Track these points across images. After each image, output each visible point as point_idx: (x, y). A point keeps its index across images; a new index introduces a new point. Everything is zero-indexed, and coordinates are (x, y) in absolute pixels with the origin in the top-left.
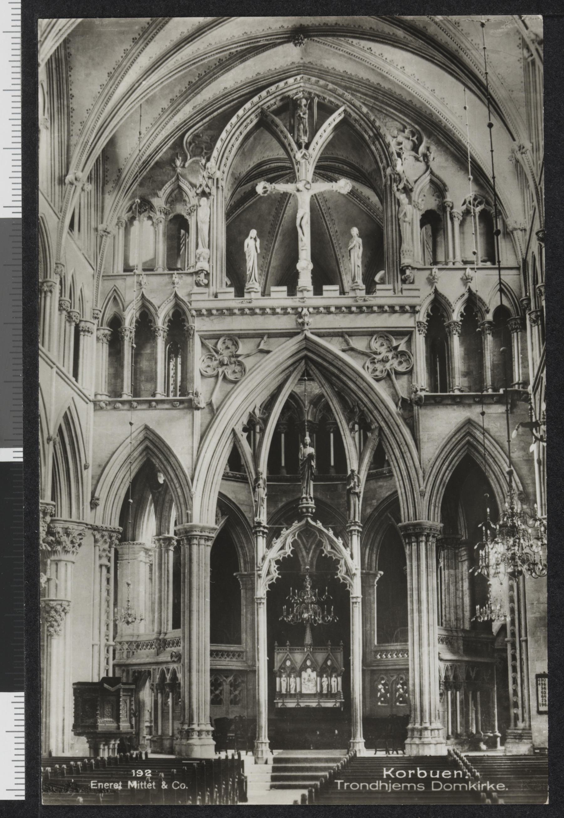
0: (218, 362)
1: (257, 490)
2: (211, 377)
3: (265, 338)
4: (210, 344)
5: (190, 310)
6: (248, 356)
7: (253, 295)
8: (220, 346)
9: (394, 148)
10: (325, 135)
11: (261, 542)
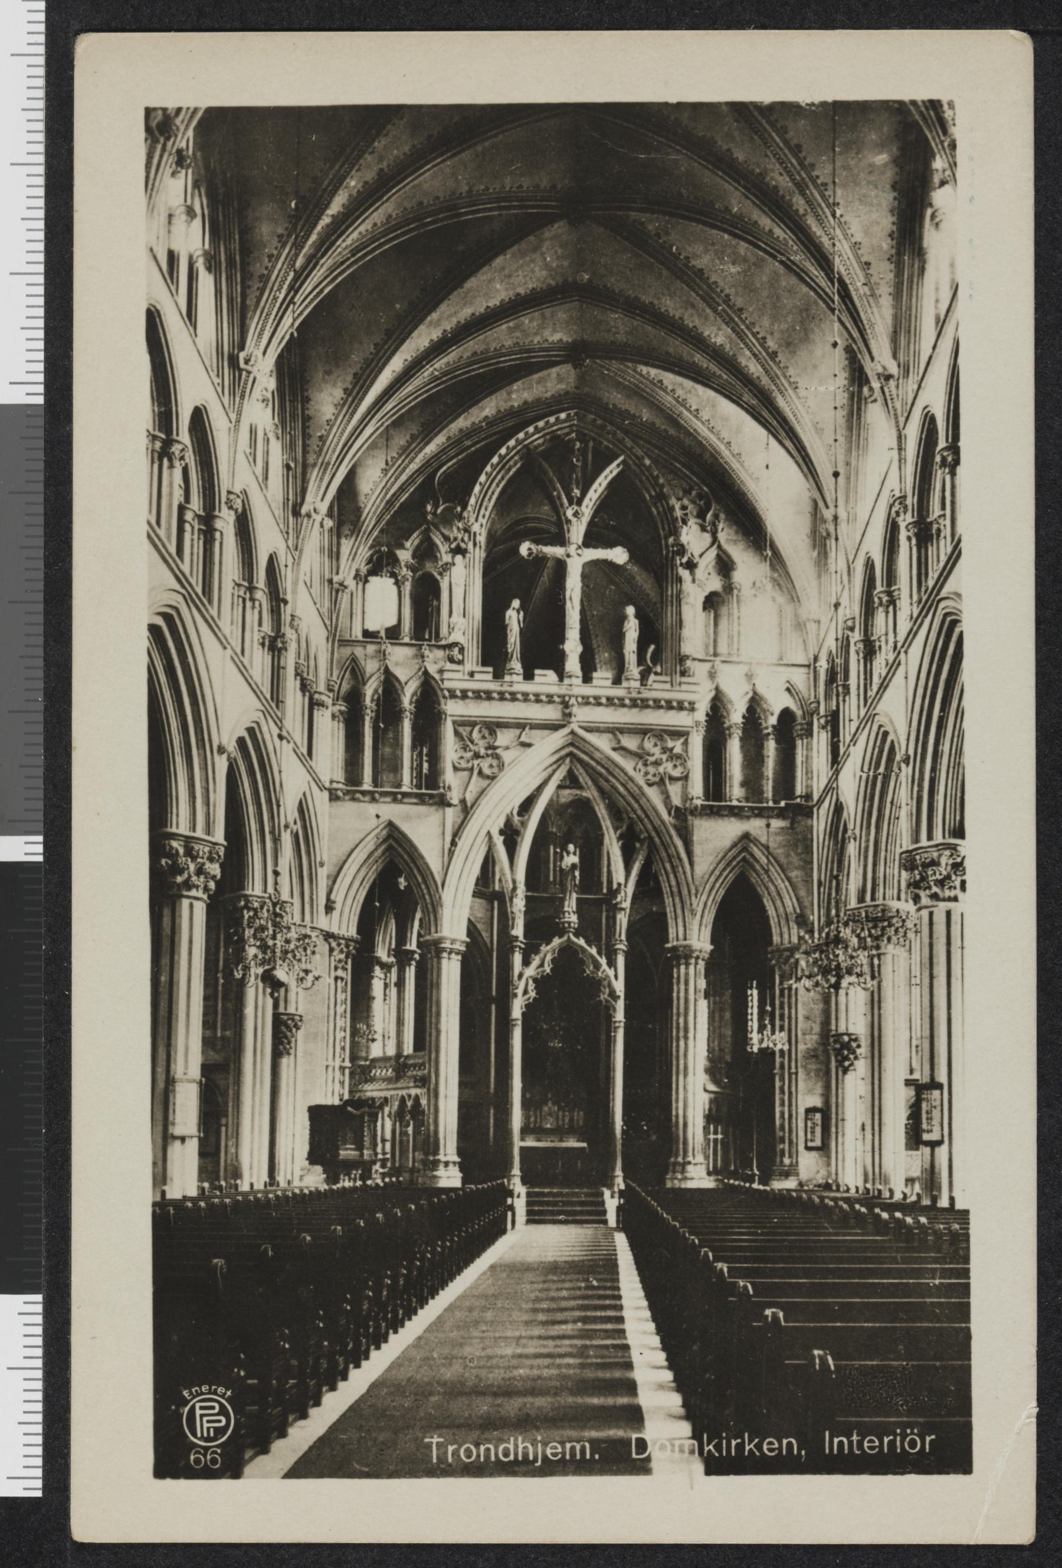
0: (471, 754)
1: (515, 900)
2: (464, 770)
3: (527, 729)
4: (464, 731)
5: (442, 690)
6: (507, 748)
7: (515, 678)
8: (476, 735)
9: (678, 513)
10: (600, 490)
11: (517, 958)
